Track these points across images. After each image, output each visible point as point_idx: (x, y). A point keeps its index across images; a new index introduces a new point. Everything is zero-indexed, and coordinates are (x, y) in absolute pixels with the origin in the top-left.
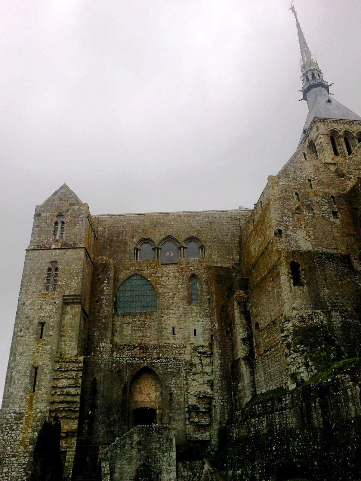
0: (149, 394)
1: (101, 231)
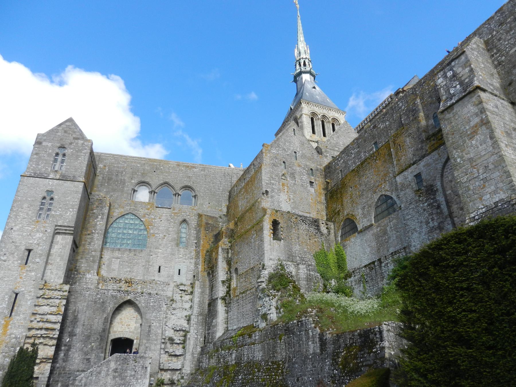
0: (129, 325)
1: (101, 168)
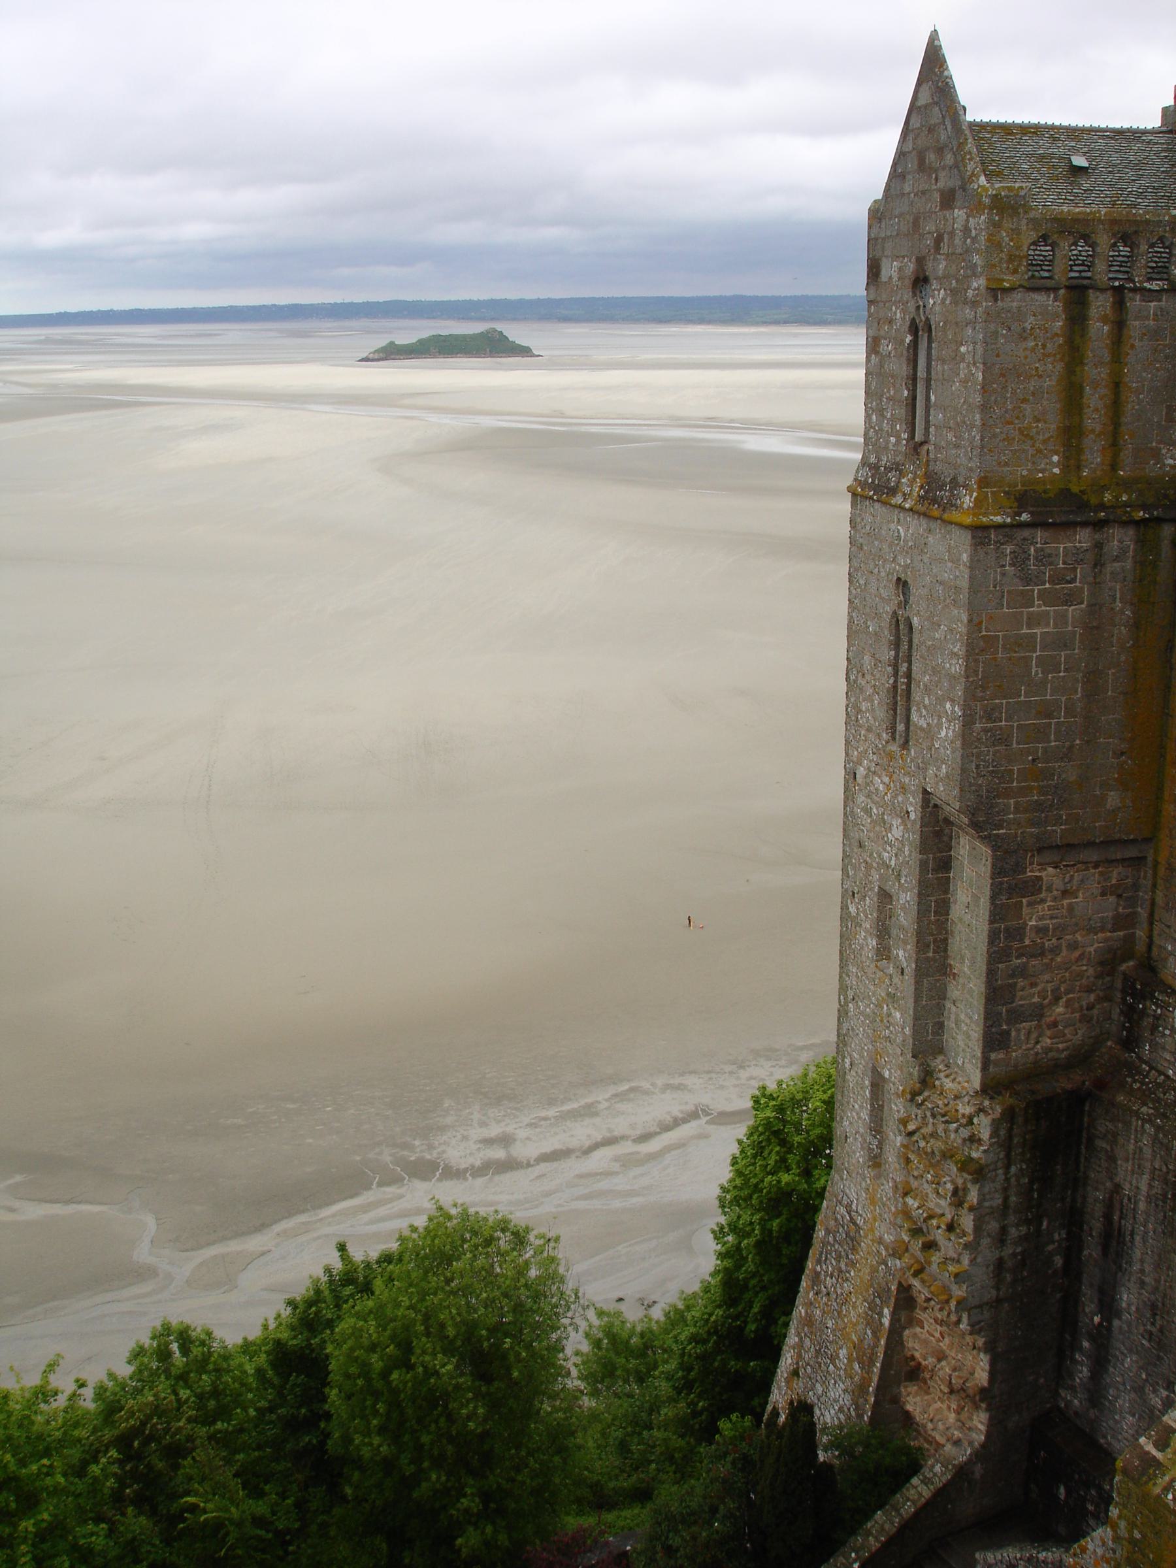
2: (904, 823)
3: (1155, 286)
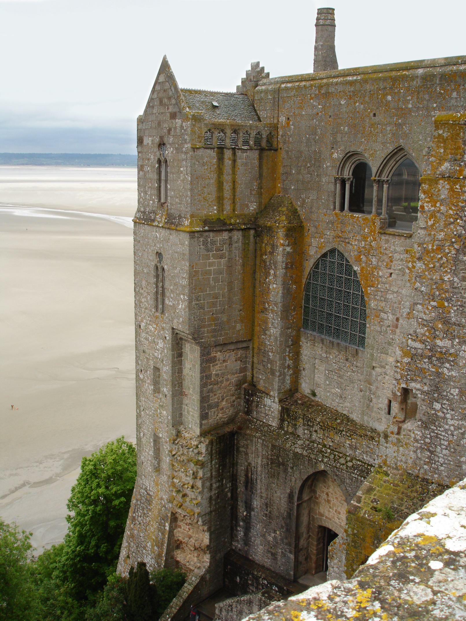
1: (283, 127)
2: (163, 340)
3: (245, 148)
